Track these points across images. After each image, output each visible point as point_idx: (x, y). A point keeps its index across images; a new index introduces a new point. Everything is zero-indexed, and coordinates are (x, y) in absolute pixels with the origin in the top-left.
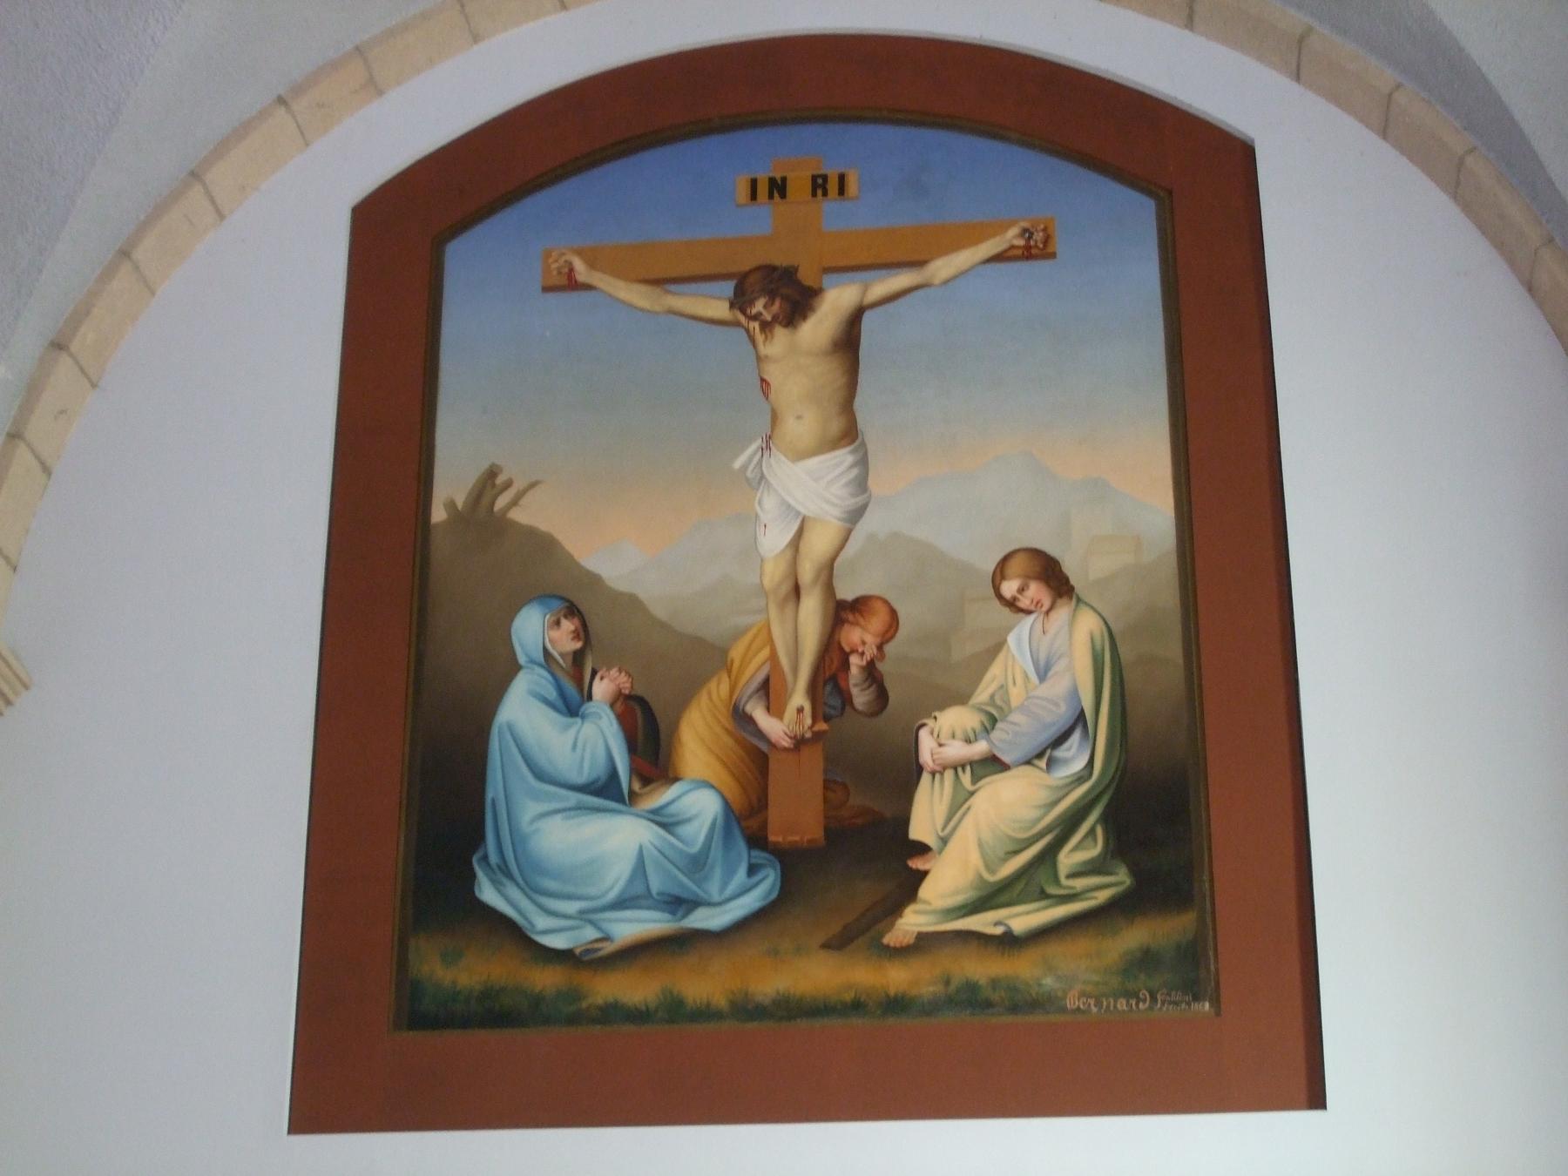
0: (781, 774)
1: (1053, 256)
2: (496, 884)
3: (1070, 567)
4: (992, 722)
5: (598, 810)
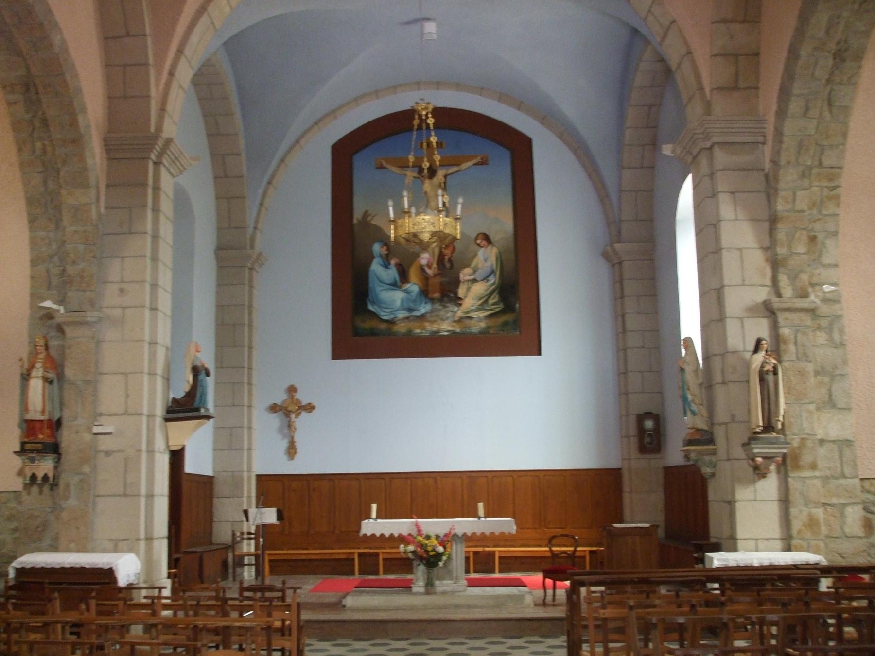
0: (431, 282)
1: (487, 164)
2: (373, 306)
3: (491, 236)
4: (475, 271)
5: (395, 289)
